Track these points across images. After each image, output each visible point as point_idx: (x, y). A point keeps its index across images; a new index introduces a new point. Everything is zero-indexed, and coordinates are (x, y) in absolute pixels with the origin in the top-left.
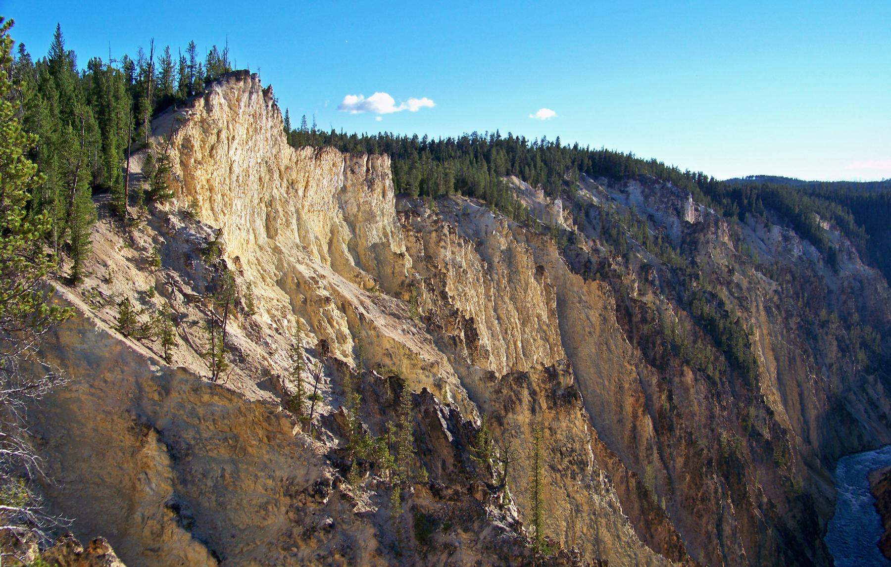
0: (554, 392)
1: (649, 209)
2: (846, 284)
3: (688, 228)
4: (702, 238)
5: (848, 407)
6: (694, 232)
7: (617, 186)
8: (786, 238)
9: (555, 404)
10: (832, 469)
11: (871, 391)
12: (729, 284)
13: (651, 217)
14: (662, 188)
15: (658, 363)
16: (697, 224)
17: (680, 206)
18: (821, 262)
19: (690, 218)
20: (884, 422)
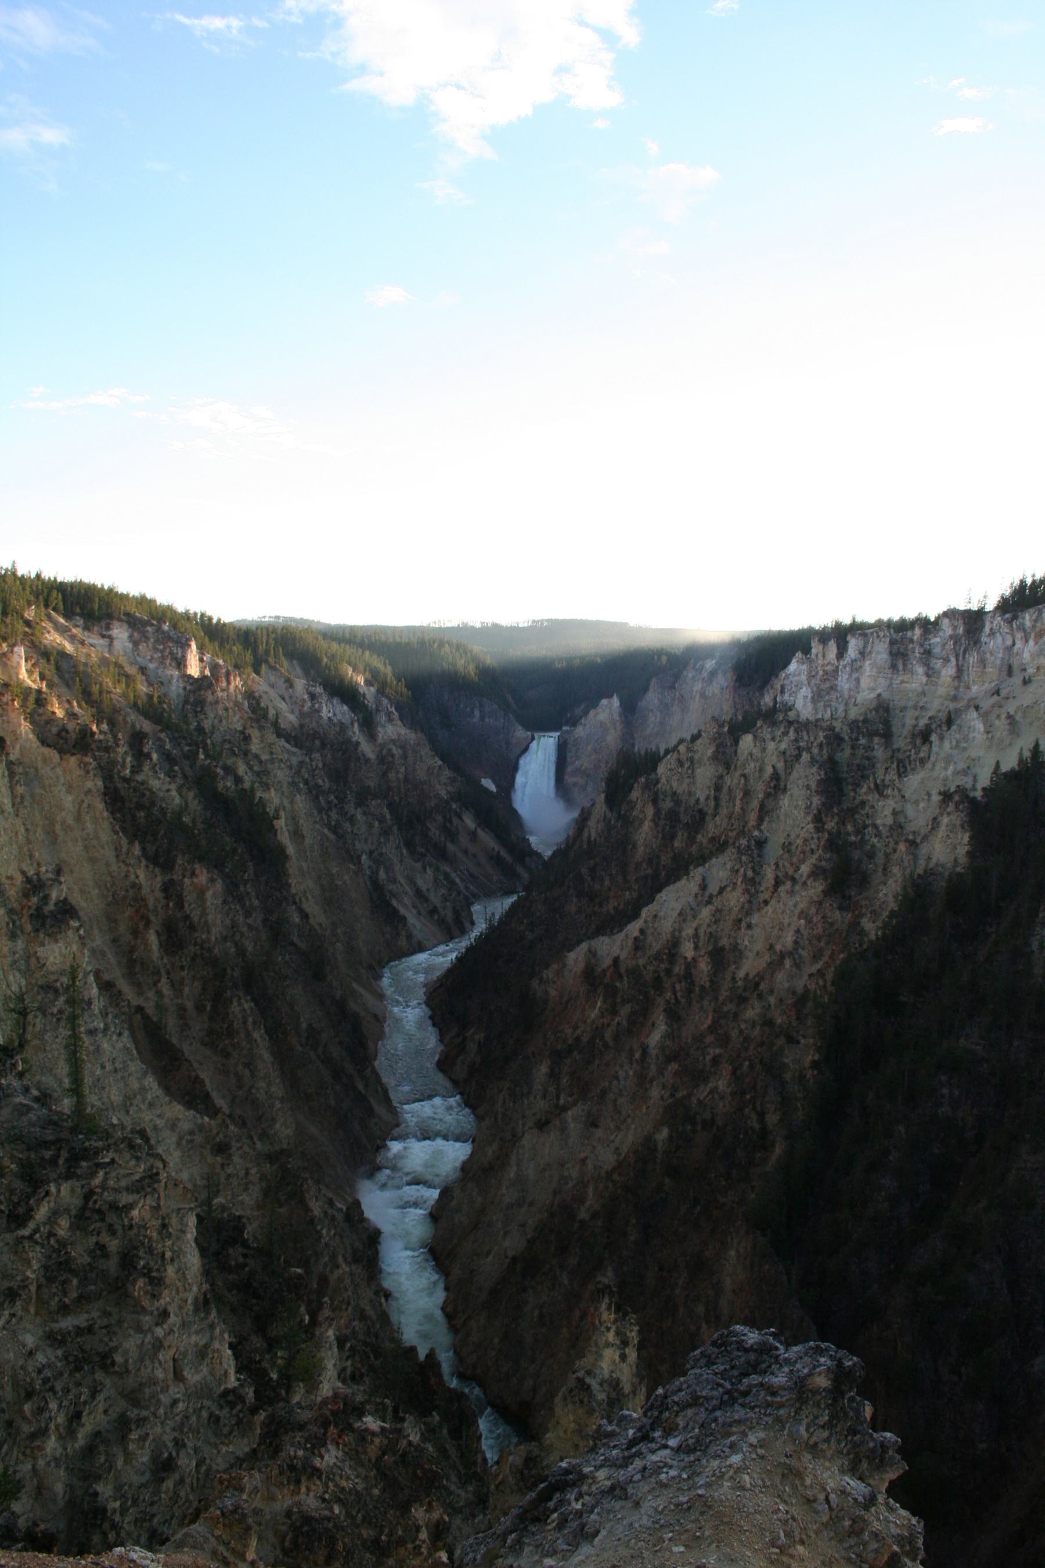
0: (39, 909)
1: (139, 659)
2: (384, 752)
3: (191, 684)
4: (210, 698)
5: (394, 903)
6: (200, 689)
7: (96, 629)
8: (313, 697)
9: (43, 925)
10: (379, 977)
11: (420, 882)
12: (246, 753)
13: (143, 670)
14: (157, 631)
15: (161, 860)
16: (204, 678)
17: (180, 655)
18: (356, 725)
19: (194, 669)
20: (436, 917)
